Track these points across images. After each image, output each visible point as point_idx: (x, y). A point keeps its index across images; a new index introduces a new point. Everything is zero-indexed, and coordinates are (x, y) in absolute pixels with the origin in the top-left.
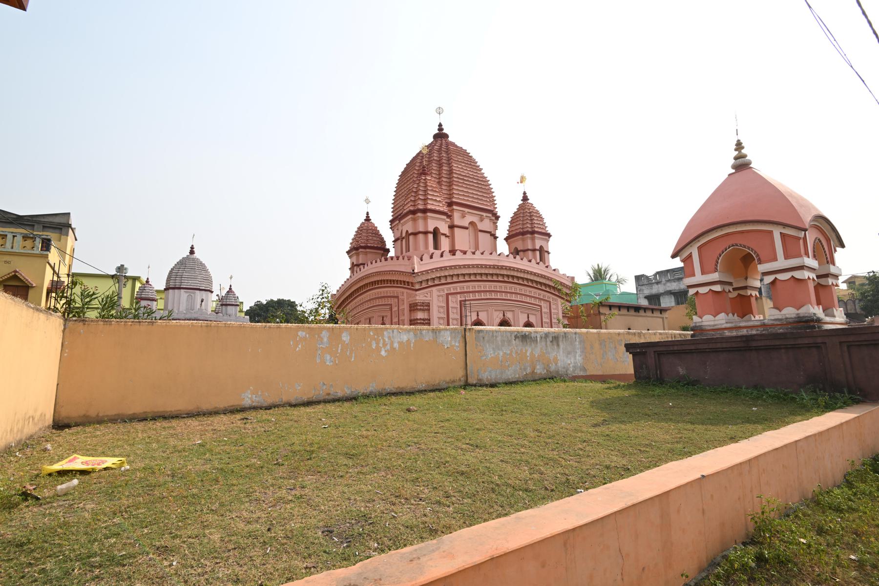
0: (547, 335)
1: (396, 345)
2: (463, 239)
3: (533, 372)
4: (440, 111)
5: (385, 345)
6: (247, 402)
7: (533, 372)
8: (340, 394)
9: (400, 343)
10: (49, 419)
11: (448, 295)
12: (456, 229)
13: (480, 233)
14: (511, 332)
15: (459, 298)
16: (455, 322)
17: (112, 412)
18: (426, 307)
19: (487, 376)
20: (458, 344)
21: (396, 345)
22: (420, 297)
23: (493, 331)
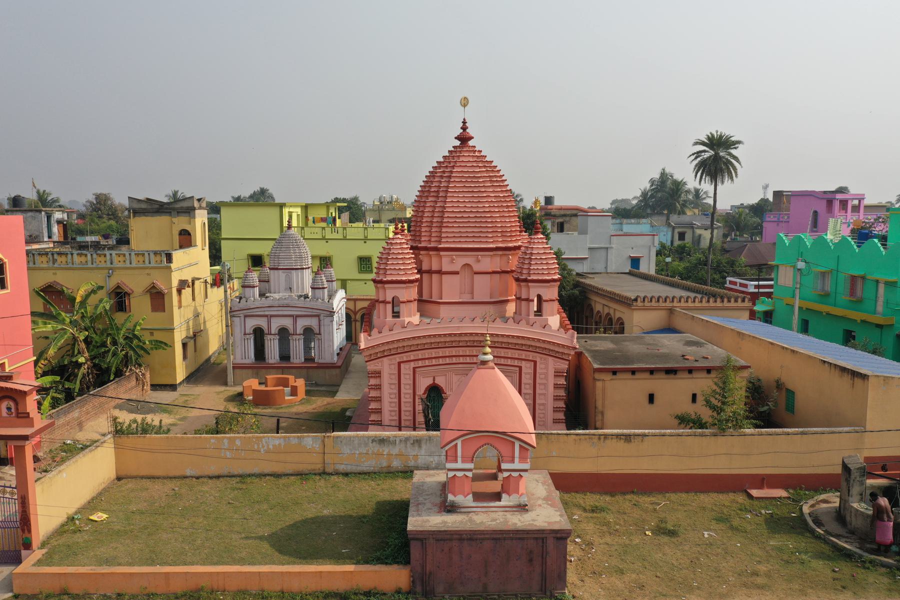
0: (407, 439)
1: (271, 447)
2: (451, 289)
3: (389, 466)
4: (465, 103)
5: (263, 447)
6: (188, 474)
7: (389, 466)
8: (236, 473)
9: (274, 446)
10: (113, 475)
11: (399, 363)
12: (444, 276)
13: (475, 276)
14: (369, 437)
15: (412, 365)
16: (408, 387)
17: (135, 474)
18: (378, 374)
19: (342, 468)
20: (317, 446)
21: (271, 447)
22: (372, 367)
23: (350, 437)
